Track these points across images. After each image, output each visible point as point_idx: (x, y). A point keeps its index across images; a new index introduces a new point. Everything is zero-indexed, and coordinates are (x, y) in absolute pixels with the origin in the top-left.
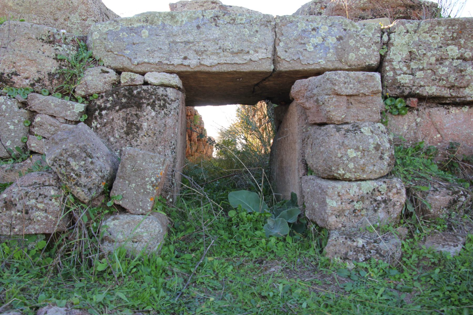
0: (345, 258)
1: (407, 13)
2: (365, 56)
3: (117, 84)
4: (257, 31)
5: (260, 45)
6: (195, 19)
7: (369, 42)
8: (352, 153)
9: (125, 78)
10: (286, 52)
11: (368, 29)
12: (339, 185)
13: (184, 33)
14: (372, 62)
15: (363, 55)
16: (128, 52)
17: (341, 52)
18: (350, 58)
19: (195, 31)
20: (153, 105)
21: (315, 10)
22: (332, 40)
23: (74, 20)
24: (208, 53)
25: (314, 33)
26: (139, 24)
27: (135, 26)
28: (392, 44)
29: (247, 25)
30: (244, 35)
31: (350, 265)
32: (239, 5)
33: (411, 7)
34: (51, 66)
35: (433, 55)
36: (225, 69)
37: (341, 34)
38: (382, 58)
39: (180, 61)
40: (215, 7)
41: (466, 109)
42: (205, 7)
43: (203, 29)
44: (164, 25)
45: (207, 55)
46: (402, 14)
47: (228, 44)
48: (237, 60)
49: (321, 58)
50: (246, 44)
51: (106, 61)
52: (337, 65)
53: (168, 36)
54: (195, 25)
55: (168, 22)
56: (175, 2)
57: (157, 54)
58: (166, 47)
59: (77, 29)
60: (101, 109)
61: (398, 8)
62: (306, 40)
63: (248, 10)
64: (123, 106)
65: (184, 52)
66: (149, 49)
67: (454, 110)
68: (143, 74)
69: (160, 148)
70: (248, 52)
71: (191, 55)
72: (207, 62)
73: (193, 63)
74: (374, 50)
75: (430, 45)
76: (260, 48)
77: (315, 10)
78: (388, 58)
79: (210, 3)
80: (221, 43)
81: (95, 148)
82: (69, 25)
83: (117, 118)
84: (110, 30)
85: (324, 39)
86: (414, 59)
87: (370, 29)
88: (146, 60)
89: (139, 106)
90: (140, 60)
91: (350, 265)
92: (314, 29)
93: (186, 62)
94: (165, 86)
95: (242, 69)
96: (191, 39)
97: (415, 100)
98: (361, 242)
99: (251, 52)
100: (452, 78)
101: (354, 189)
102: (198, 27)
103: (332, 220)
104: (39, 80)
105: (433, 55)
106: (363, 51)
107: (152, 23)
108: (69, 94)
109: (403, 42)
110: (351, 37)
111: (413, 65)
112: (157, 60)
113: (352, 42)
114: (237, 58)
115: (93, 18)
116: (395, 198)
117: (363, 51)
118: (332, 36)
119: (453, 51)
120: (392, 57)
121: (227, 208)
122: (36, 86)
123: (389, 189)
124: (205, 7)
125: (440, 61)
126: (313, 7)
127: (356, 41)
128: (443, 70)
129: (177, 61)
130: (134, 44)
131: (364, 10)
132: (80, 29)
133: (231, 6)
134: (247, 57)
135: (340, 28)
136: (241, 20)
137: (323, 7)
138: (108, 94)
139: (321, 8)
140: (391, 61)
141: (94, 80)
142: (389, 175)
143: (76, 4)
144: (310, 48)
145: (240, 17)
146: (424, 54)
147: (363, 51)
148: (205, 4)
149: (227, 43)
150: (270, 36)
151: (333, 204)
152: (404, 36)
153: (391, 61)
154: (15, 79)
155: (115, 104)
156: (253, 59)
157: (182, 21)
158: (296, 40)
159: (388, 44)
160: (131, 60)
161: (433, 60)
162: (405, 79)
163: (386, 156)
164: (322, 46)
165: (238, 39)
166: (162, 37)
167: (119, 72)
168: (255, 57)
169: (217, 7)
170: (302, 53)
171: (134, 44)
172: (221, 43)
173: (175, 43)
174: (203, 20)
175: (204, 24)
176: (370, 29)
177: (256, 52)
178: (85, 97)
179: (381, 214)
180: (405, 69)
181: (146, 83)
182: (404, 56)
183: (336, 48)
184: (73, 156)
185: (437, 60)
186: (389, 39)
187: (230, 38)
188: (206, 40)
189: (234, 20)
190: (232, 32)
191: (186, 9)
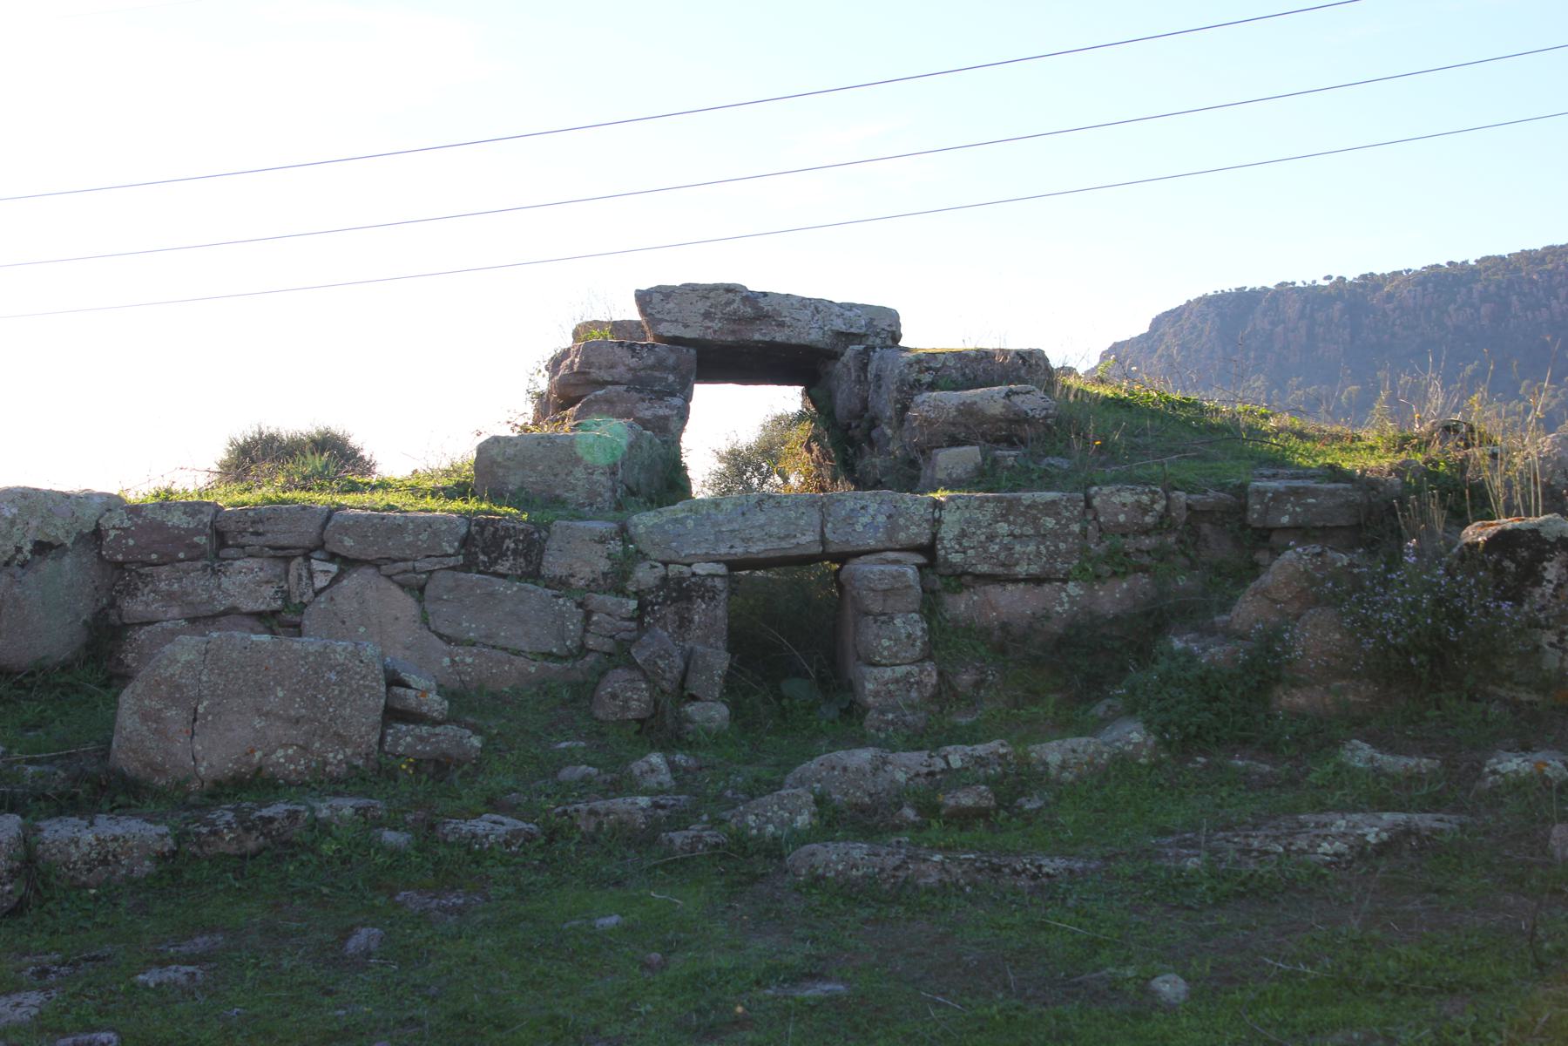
0: (878, 730)
2: (916, 535)
3: (665, 579)
8: (886, 643)
9: (674, 570)
12: (876, 671)
17: (892, 529)
19: (740, 519)
20: (703, 598)
22: (881, 519)
23: (579, 475)
31: (882, 736)
32: (783, 292)
33: (1017, 422)
34: (604, 565)
36: (772, 554)
38: (934, 536)
41: (1021, 586)
44: (709, 515)
47: (774, 530)
48: (784, 544)
51: (653, 555)
52: (888, 545)
53: (713, 525)
55: (712, 511)
56: (644, 287)
60: (654, 605)
64: (674, 601)
67: (1010, 587)
68: (689, 565)
69: (712, 640)
71: (737, 542)
72: (754, 549)
73: (739, 550)
81: (660, 645)
83: (669, 612)
85: (874, 517)
87: (922, 504)
89: (690, 599)
91: (882, 736)
94: (713, 576)
97: (969, 578)
98: (890, 716)
100: (1002, 556)
101: (888, 673)
103: (870, 700)
104: (594, 580)
108: (621, 592)
110: (901, 515)
111: (965, 543)
113: (902, 521)
116: (926, 680)
119: (1003, 528)
121: (779, 698)
122: (593, 586)
123: (921, 672)
125: (991, 538)
128: (994, 548)
129: (723, 550)
131: (954, 424)
133: (765, 294)
138: (659, 588)
139: (920, 372)
140: (942, 539)
141: (645, 575)
142: (922, 660)
144: (859, 528)
150: (816, 517)
151: (870, 686)
153: (942, 539)
154: (572, 580)
155: (666, 598)
159: (937, 522)
161: (983, 538)
162: (956, 558)
163: (918, 643)
164: (870, 525)
167: (666, 564)
168: (803, 540)
176: (922, 504)
178: (636, 593)
179: (914, 694)
181: (694, 574)
184: (660, 657)
191: (671, 305)
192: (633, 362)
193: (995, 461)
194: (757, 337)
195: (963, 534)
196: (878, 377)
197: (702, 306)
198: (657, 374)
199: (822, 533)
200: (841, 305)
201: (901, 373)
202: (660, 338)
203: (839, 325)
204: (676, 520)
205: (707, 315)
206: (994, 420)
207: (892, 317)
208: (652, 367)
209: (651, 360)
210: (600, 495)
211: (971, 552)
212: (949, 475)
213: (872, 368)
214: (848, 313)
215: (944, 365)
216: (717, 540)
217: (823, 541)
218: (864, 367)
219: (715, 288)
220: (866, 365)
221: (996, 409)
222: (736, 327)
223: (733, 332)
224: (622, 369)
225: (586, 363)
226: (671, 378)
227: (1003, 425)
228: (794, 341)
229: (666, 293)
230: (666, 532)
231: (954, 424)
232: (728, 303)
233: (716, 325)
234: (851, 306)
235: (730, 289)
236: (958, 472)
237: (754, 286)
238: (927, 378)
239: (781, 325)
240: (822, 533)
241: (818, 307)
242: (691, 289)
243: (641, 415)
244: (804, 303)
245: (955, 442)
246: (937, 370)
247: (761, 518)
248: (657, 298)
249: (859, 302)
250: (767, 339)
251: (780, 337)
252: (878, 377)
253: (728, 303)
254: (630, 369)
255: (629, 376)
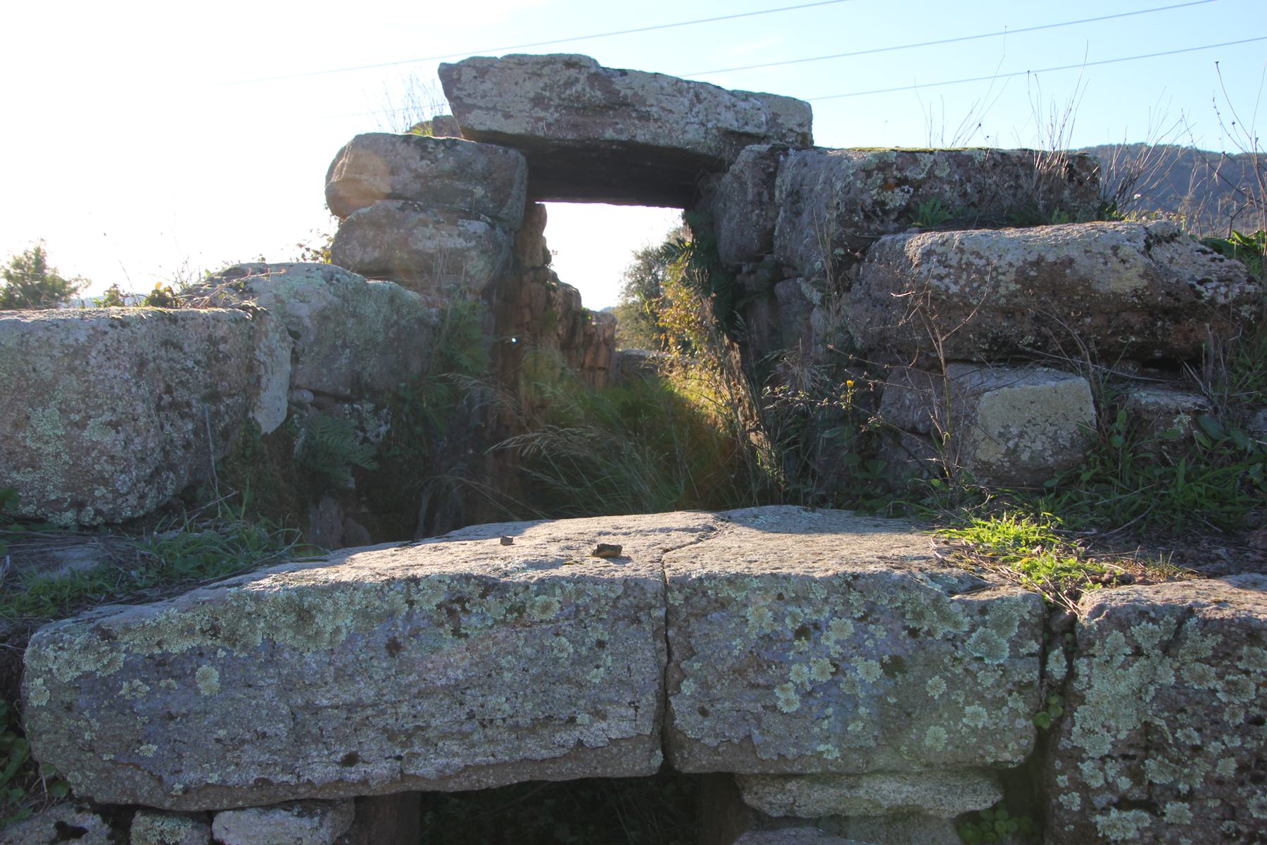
1: (1153, 334)
2: (985, 735)
4: (601, 644)
5: (612, 694)
6: (380, 619)
7: (998, 685)
10: (704, 713)
11: (997, 626)
13: (342, 676)
14: (1007, 756)
15: (974, 731)
16: (149, 750)
18: (928, 742)
19: (382, 665)
21: (865, 196)
22: (866, 672)
23: (45, 428)
24: (430, 734)
25: (803, 645)
26: (186, 644)
27: (175, 649)
28: (1082, 700)
29: (564, 625)
30: (556, 661)
32: (650, 69)
33: (1166, 312)
35: (1228, 753)
36: (491, 781)
37: (897, 650)
38: (1045, 741)
39: (332, 772)
40: (577, 80)
42: (546, 80)
43: (412, 651)
44: (273, 648)
45: (427, 741)
46: (1137, 334)
47: (498, 703)
48: (533, 748)
49: (826, 739)
50: (562, 690)
53: (287, 688)
54: (382, 640)
56: (454, 60)
57: (250, 754)
58: (282, 728)
59: (57, 455)
61: (1124, 315)
62: (773, 671)
63: (678, 81)
65: (344, 739)
66: (222, 733)
70: (572, 720)
71: (370, 744)
74: (1014, 713)
75: (1220, 709)
76: (611, 702)
77: (865, 196)
78: (1064, 743)
79: (559, 66)
80: (473, 700)
82: (28, 443)
84: (88, 675)
85: (839, 667)
86: (1161, 748)
88: (214, 778)
90: (192, 776)
92: (802, 632)
93: (354, 774)
95: (551, 775)
96: (369, 694)
99: (583, 718)
102: (394, 647)
105: (1228, 753)
106: (977, 715)
107: (232, 639)
109: (1122, 688)
110: (933, 665)
112: (254, 775)
113: (936, 686)
114: (530, 743)
115: (108, 416)
117: (977, 715)
118: (867, 656)
120: (1080, 742)
124: (546, 80)
126: (859, 184)
127: (952, 683)
129: (321, 769)
130: (171, 717)
132: (65, 457)
133: (623, 73)
134: (567, 737)
135: (897, 625)
136: (546, 608)
137: (891, 181)
139: (885, 186)
140: (1076, 756)
143: (49, 375)
144: (787, 700)
145: (541, 599)
146: (1196, 749)
147: (976, 716)
148: (546, 70)
149: (492, 701)
150: (645, 661)
152: (1124, 666)
153: (1076, 756)
156: (589, 740)
157: (337, 630)
158: (740, 672)
159: (1064, 693)
160: (160, 779)
161: (1228, 768)
165: (535, 679)
166: (268, 693)
168: (596, 732)
169: (583, 78)
170: (758, 719)
171: (171, 717)
172: (473, 700)
173: (316, 711)
174: (409, 617)
175: (415, 634)
177: (600, 715)
180: (1124, 783)
182: (1123, 735)
183: (880, 700)
185: (1242, 768)
186: (1071, 674)
187: (507, 676)
188: (421, 695)
189: (520, 609)
190: (514, 653)
191: (488, 85)
192: (422, 166)
193: (1139, 422)
194: (609, 134)
195: (1147, 741)
196: (795, 195)
197: (531, 88)
198: (459, 185)
199: (664, 714)
200: (733, 94)
201: (848, 188)
202: (470, 132)
203: (729, 121)
204: (161, 664)
205: (538, 101)
206: (1116, 306)
207: (802, 111)
208: (452, 174)
209: (449, 164)
210: (104, 482)
211: (1172, 809)
212: (1013, 453)
213: (784, 182)
214: (742, 105)
215: (931, 175)
216: (299, 738)
217: (666, 734)
218: (769, 180)
219: (551, 60)
220: (772, 176)
221: (1126, 280)
222: (580, 120)
223: (575, 126)
224: (406, 176)
225: (356, 167)
226: (479, 191)
227: (1136, 320)
228: (662, 142)
229: (480, 67)
230: (125, 708)
231: (1008, 313)
232: (569, 83)
233: (551, 116)
234: (747, 96)
235: (573, 62)
236: (1036, 447)
237: (609, 59)
238: (897, 199)
239: (645, 117)
240: (664, 714)
241: (700, 93)
242: (518, 61)
243: (420, 246)
244: (679, 86)
245: (1008, 355)
246: (917, 185)
247: (451, 659)
248: (468, 74)
249: (756, 89)
250: (624, 138)
251: (642, 135)
252: (795, 195)
253: (569, 83)
254: (418, 176)
255: (416, 186)
